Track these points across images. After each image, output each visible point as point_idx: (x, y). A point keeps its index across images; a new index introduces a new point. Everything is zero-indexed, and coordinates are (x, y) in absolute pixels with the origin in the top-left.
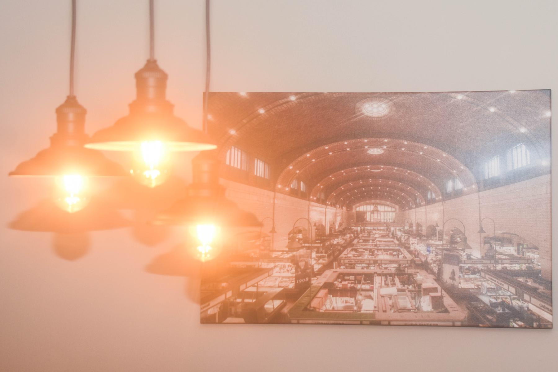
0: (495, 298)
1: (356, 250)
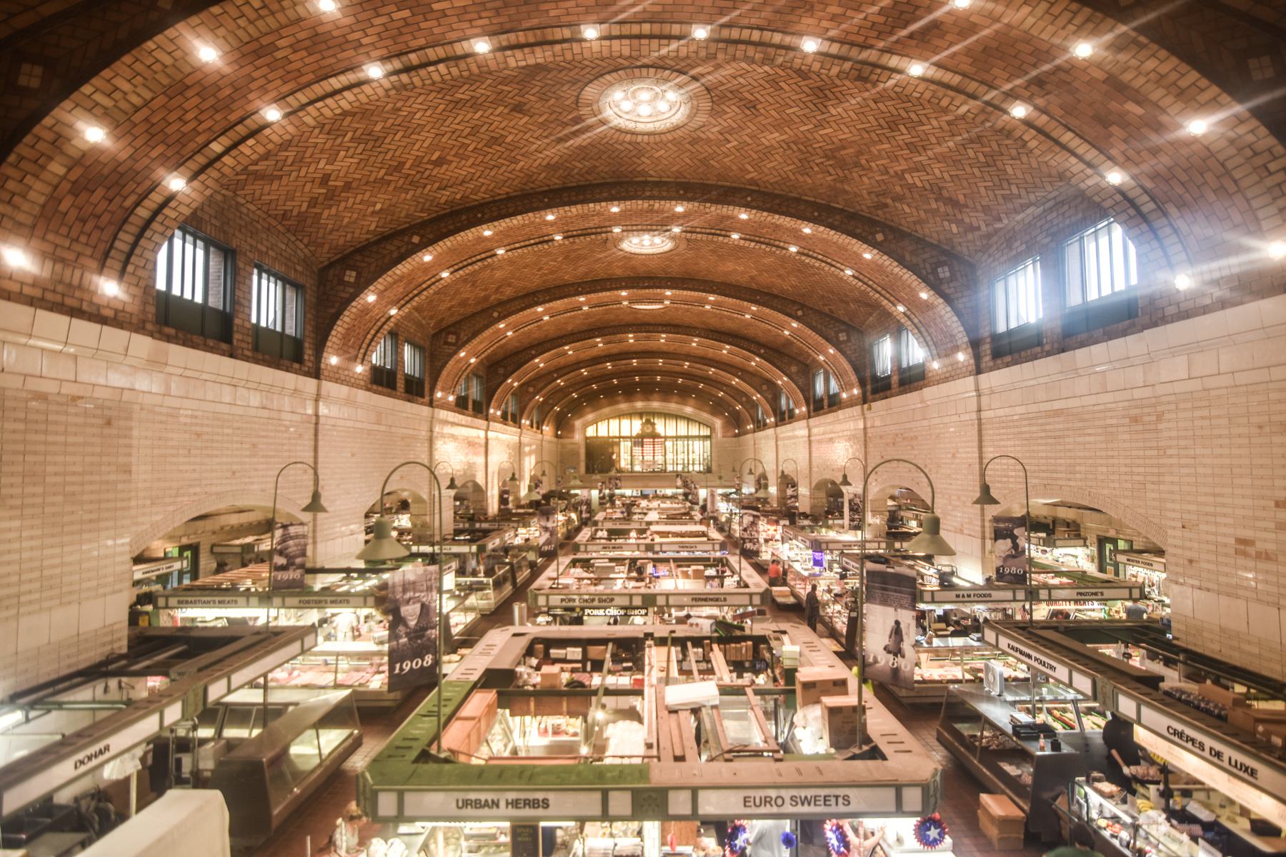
0: (1028, 711)
1: (586, 564)
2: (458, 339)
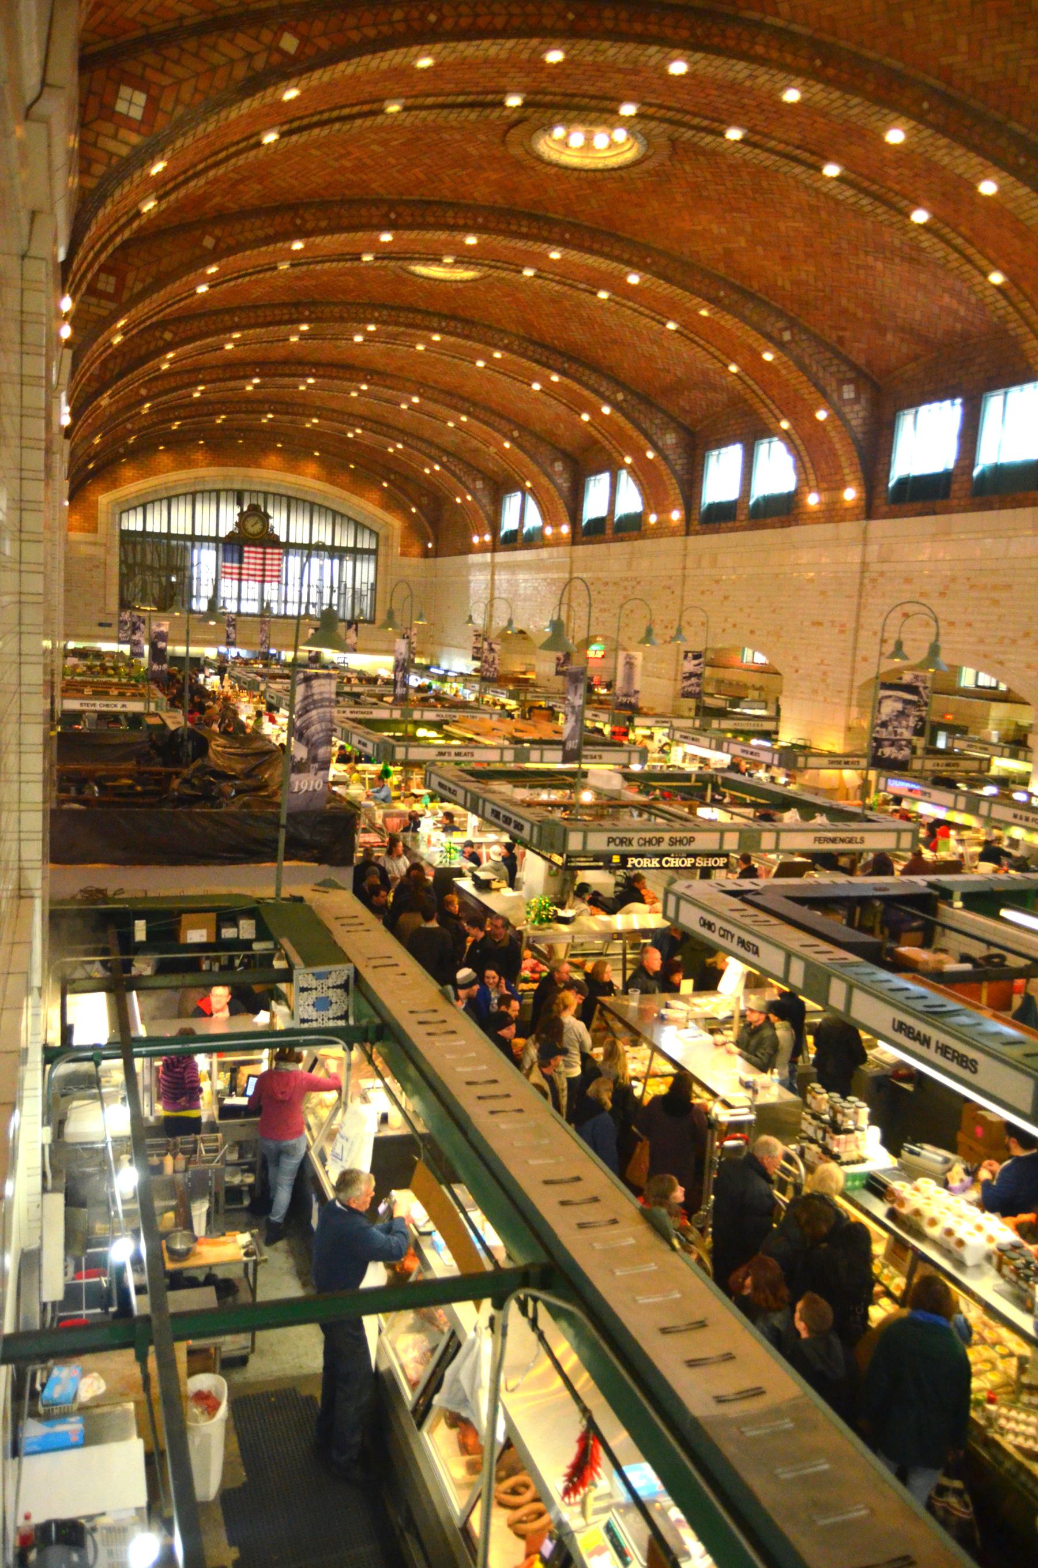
2: (120, 286)
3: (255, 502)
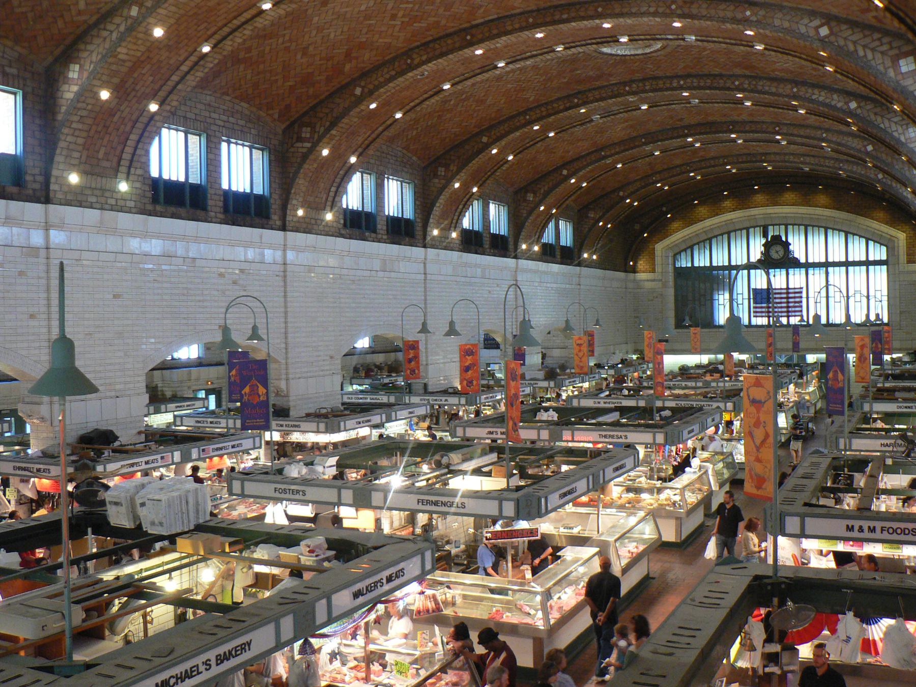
3: (777, 233)
